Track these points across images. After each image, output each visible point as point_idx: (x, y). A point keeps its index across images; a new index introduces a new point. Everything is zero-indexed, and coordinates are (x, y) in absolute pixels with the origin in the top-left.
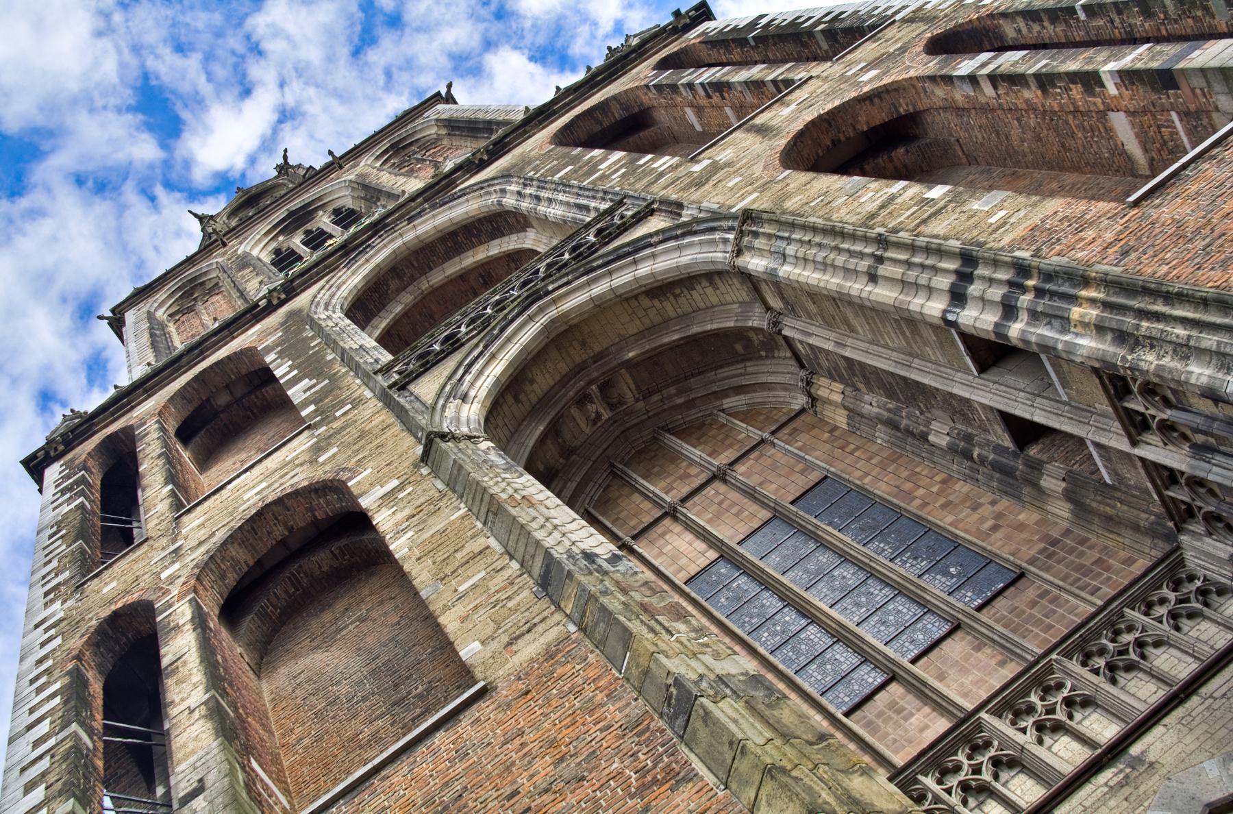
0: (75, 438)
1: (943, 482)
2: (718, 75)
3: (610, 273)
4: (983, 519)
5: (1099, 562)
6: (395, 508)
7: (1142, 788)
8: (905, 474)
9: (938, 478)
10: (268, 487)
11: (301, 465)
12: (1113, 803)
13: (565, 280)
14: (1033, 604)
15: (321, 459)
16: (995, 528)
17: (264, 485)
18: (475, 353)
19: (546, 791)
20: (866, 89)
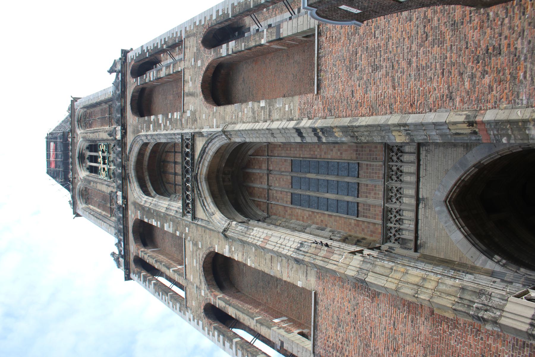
0: (127, 266)
1: (318, 147)
2: (155, 75)
3: (204, 159)
4: (336, 153)
5: (370, 151)
6: (236, 254)
7: (430, 204)
8: (308, 150)
9: (316, 147)
10: (197, 260)
11: (197, 250)
12: (427, 211)
13: (197, 168)
14: (367, 169)
15: (200, 247)
16: (341, 154)
17: (195, 261)
18: (201, 201)
19: (354, 309)
20: (204, 69)
